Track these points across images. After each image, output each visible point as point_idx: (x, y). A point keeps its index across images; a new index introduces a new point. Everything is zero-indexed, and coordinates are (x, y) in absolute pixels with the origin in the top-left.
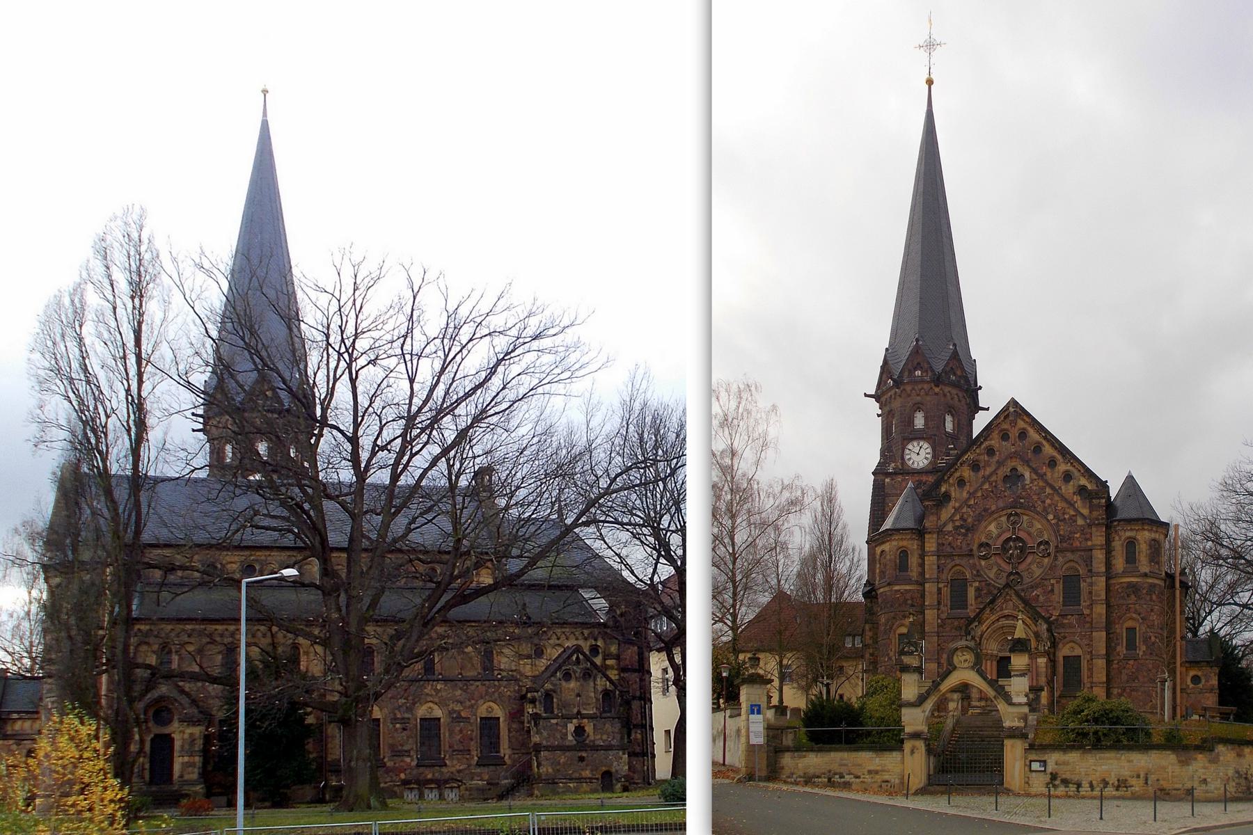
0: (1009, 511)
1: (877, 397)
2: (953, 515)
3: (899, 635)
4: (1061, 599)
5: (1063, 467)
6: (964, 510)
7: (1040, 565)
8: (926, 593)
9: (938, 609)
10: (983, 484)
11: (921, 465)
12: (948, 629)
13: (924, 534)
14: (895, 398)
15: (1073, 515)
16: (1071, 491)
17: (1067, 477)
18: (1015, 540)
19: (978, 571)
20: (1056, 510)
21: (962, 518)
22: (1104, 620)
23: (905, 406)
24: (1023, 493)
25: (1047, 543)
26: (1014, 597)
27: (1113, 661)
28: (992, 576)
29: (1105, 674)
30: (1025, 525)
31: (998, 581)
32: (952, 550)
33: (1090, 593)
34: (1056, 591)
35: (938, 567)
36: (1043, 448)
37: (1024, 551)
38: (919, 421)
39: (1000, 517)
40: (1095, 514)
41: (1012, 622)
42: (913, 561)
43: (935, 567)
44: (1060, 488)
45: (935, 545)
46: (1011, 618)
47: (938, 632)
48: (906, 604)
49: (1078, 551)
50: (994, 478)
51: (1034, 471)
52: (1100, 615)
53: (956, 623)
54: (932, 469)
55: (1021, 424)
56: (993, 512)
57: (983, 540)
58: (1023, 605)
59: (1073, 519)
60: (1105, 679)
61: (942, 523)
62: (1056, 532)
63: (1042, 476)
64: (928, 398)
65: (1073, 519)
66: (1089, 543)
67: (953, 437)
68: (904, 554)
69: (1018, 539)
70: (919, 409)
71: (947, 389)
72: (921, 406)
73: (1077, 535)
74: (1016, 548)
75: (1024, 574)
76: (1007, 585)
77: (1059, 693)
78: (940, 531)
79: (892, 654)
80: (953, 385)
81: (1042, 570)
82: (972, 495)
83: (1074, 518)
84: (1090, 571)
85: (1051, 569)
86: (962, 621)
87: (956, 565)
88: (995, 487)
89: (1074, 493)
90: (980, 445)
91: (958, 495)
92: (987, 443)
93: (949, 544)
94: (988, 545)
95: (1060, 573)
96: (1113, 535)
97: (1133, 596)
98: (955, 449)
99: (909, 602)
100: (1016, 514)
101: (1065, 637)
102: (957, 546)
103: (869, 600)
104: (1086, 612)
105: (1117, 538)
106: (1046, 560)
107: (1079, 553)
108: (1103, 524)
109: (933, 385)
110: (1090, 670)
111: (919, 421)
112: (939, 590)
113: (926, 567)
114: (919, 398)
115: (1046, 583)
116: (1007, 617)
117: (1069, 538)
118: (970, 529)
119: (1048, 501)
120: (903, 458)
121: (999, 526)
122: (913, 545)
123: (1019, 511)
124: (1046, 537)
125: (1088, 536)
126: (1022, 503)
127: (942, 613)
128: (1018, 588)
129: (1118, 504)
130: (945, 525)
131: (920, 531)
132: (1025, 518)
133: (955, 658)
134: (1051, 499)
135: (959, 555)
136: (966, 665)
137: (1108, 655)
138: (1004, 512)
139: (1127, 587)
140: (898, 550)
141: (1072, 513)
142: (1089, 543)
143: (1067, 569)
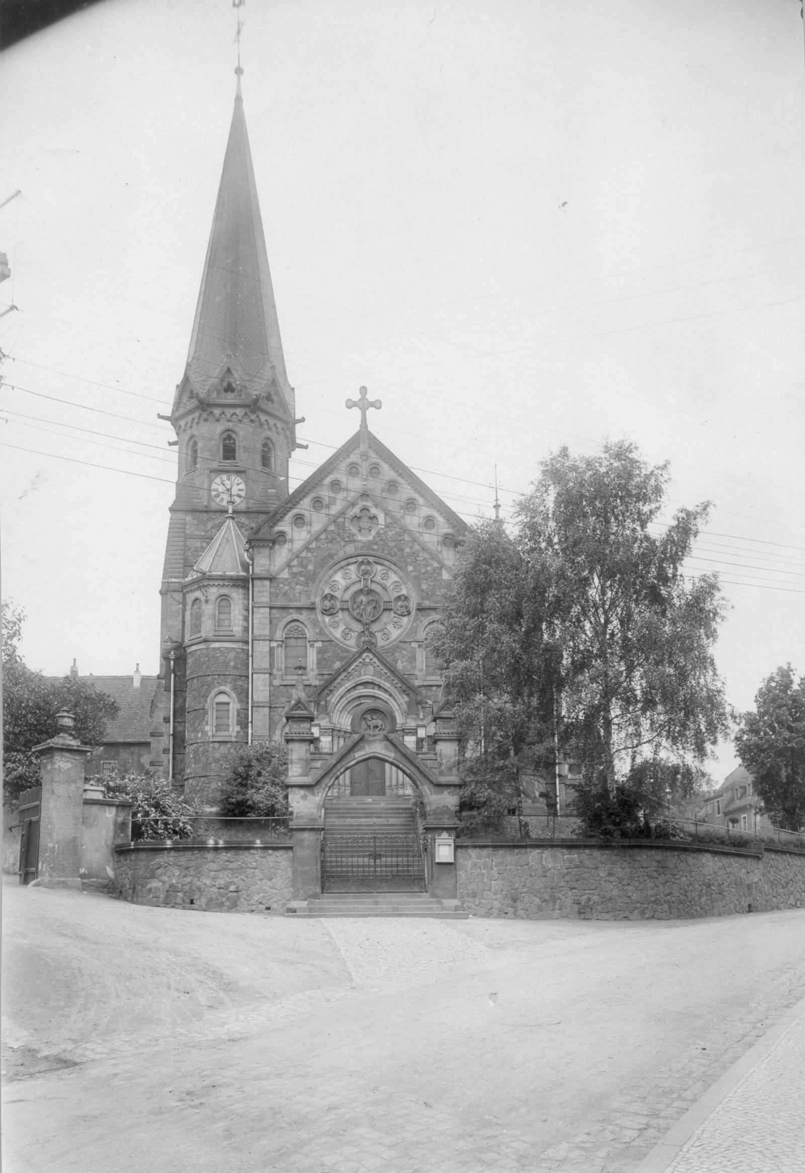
0: (360, 559)
9: (270, 674)
21: (301, 564)
25: (406, 598)
39: (348, 564)
45: (267, 594)
69: (370, 592)
81: (400, 631)
100: (369, 563)
106: (405, 619)
118: (311, 578)
123: (371, 559)
132: (379, 568)
138: (354, 560)
141: (436, 565)
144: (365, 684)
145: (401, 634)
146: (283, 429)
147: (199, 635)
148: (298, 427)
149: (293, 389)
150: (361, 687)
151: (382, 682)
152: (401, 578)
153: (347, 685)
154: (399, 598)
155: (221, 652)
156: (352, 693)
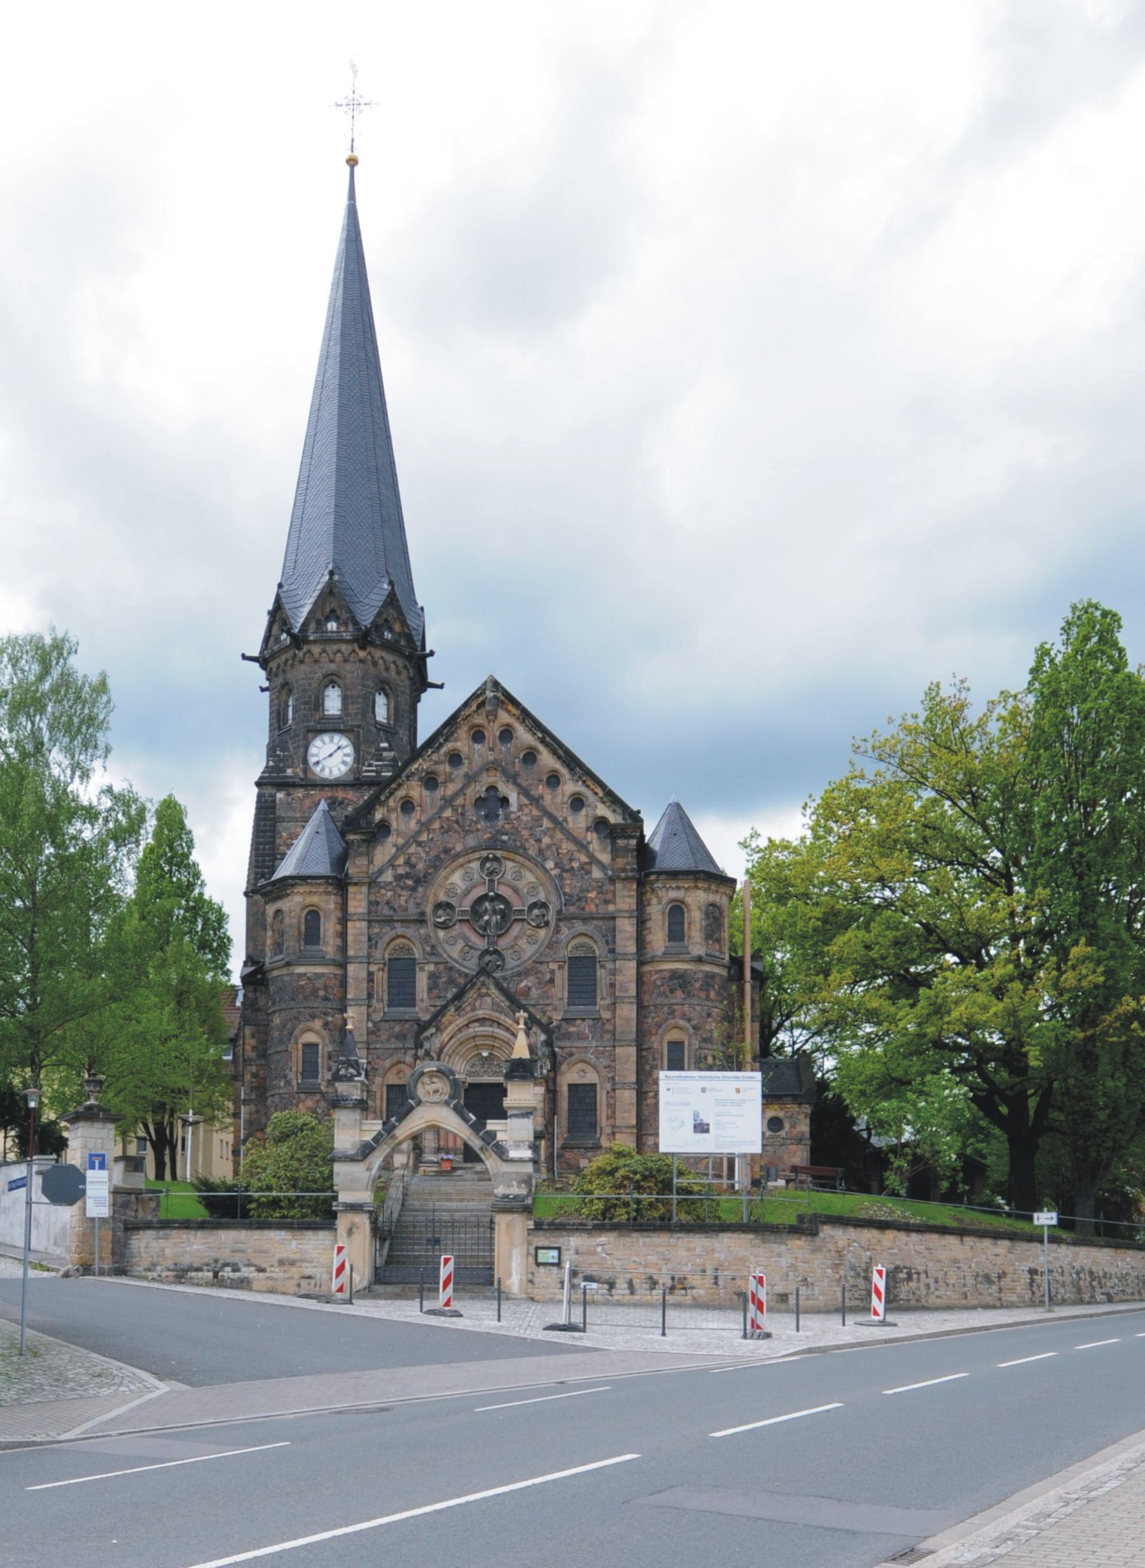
0: (484, 853)
1: (263, 661)
2: (395, 857)
3: (304, 1045)
4: (566, 994)
5: (570, 786)
6: (413, 849)
7: (532, 940)
8: (350, 980)
9: (369, 1006)
10: (442, 809)
11: (336, 774)
12: (384, 1037)
13: (347, 885)
14: (292, 666)
15: (587, 863)
16: (583, 825)
17: (577, 803)
18: (492, 900)
19: (433, 947)
20: (558, 854)
21: (408, 863)
22: (634, 1029)
23: (312, 679)
24: (507, 826)
25: (544, 905)
26: (493, 990)
27: (647, 1092)
28: (455, 955)
29: (634, 1113)
30: (509, 876)
31: (466, 963)
32: (392, 913)
33: (613, 985)
34: (558, 981)
35: (370, 939)
36: (539, 757)
37: (507, 917)
38: (333, 703)
39: (469, 862)
40: (621, 862)
41: (490, 1029)
42: (329, 927)
43: (366, 939)
44: (565, 820)
45: (364, 904)
46: (488, 1023)
47: (367, 1043)
48: (317, 997)
49: (593, 918)
50: (459, 801)
51: (524, 791)
52: (628, 1020)
53: (397, 1028)
54: (355, 782)
55: (504, 717)
56: (458, 856)
57: (442, 898)
58: (508, 1004)
59: (585, 869)
60: (634, 1122)
61: (376, 869)
62: (559, 889)
63: (536, 801)
64: (348, 667)
65: (585, 869)
66: (611, 908)
67: (387, 731)
68: (313, 917)
69: (499, 898)
70: (333, 683)
71: (378, 653)
72: (334, 678)
73: (592, 895)
74: (494, 912)
75: (507, 954)
76: (483, 971)
77: (561, 1142)
78: (373, 883)
79: (291, 1075)
80: (388, 646)
81: (535, 947)
82: (425, 826)
83: (587, 867)
84: (612, 951)
85: (552, 945)
86: (407, 1025)
87: (398, 937)
88: (463, 814)
89: (588, 829)
90: (439, 748)
91: (402, 827)
92: (449, 746)
93: (388, 903)
94: (449, 906)
95: (565, 953)
96: (649, 895)
97: (679, 992)
98: (390, 749)
99: (321, 993)
100: (496, 859)
101: (571, 1055)
102: (400, 906)
103: (251, 988)
104: (606, 1015)
105: (654, 901)
106: (542, 932)
107: (595, 922)
108: (633, 878)
109: (356, 646)
110: (612, 1106)
111: (333, 703)
112: (370, 975)
113: (350, 938)
114: (333, 666)
115: (542, 968)
116: (482, 1021)
117: (580, 899)
118: (421, 880)
119: (546, 840)
120: (305, 761)
121: (467, 876)
122: (328, 903)
123: (499, 853)
124: (542, 896)
125: (609, 896)
126: (504, 842)
127: (375, 1011)
128: (498, 974)
129: (656, 846)
130: (381, 872)
131: (339, 880)
132: (509, 864)
133: (420, 1086)
134: (552, 837)
135: (402, 921)
136: (436, 1098)
137: (639, 1083)
138: (477, 855)
139: (671, 978)
140: (303, 909)
141: (584, 859)
142: (611, 908)
143: (576, 948)
144: (482, 1021)
145: (537, 951)
146: (405, 667)
147: (280, 957)
148: (429, 660)
149: (422, 609)
150: (477, 1024)
151: (503, 1017)
152: (537, 878)
153: (457, 1022)
154: (534, 906)
155: (309, 979)
156: (464, 1033)
